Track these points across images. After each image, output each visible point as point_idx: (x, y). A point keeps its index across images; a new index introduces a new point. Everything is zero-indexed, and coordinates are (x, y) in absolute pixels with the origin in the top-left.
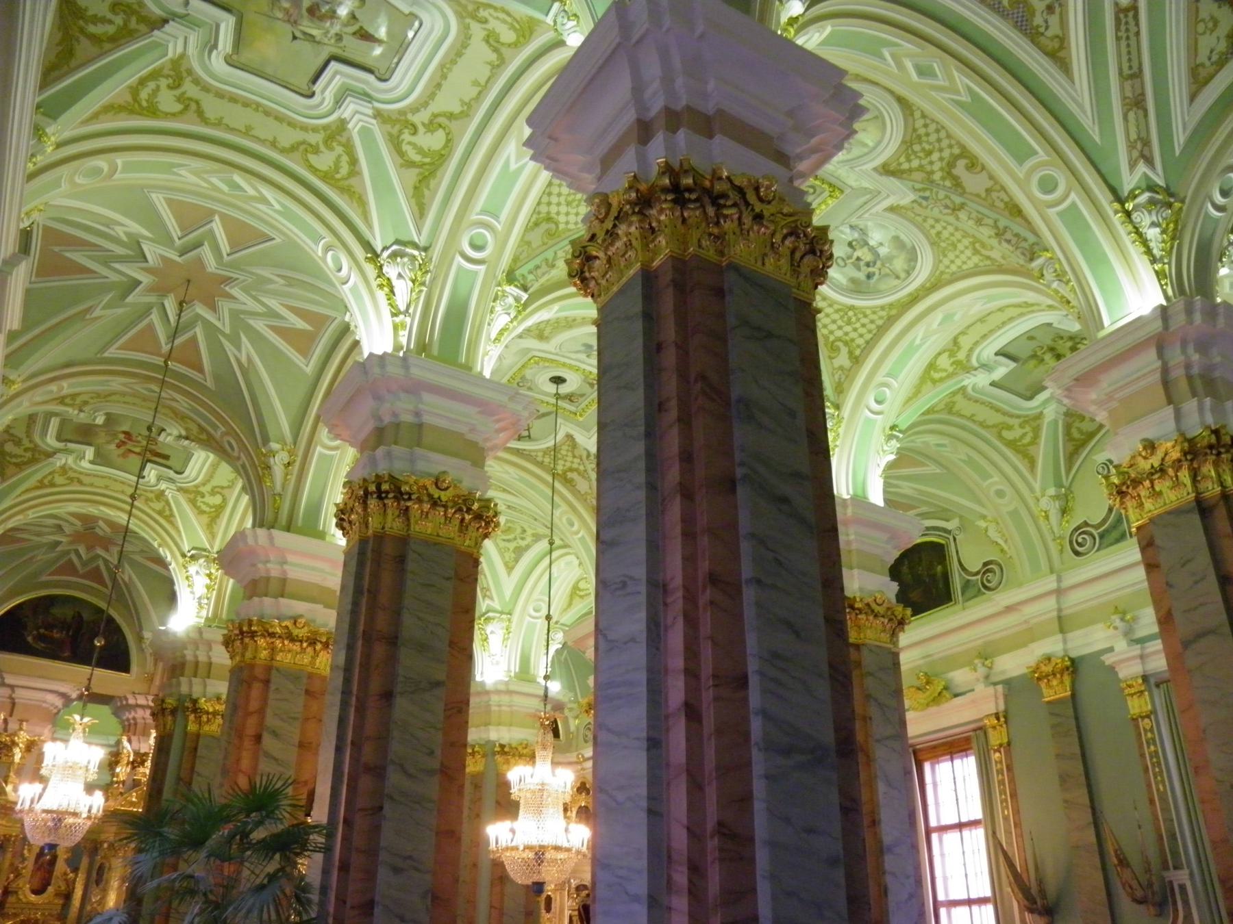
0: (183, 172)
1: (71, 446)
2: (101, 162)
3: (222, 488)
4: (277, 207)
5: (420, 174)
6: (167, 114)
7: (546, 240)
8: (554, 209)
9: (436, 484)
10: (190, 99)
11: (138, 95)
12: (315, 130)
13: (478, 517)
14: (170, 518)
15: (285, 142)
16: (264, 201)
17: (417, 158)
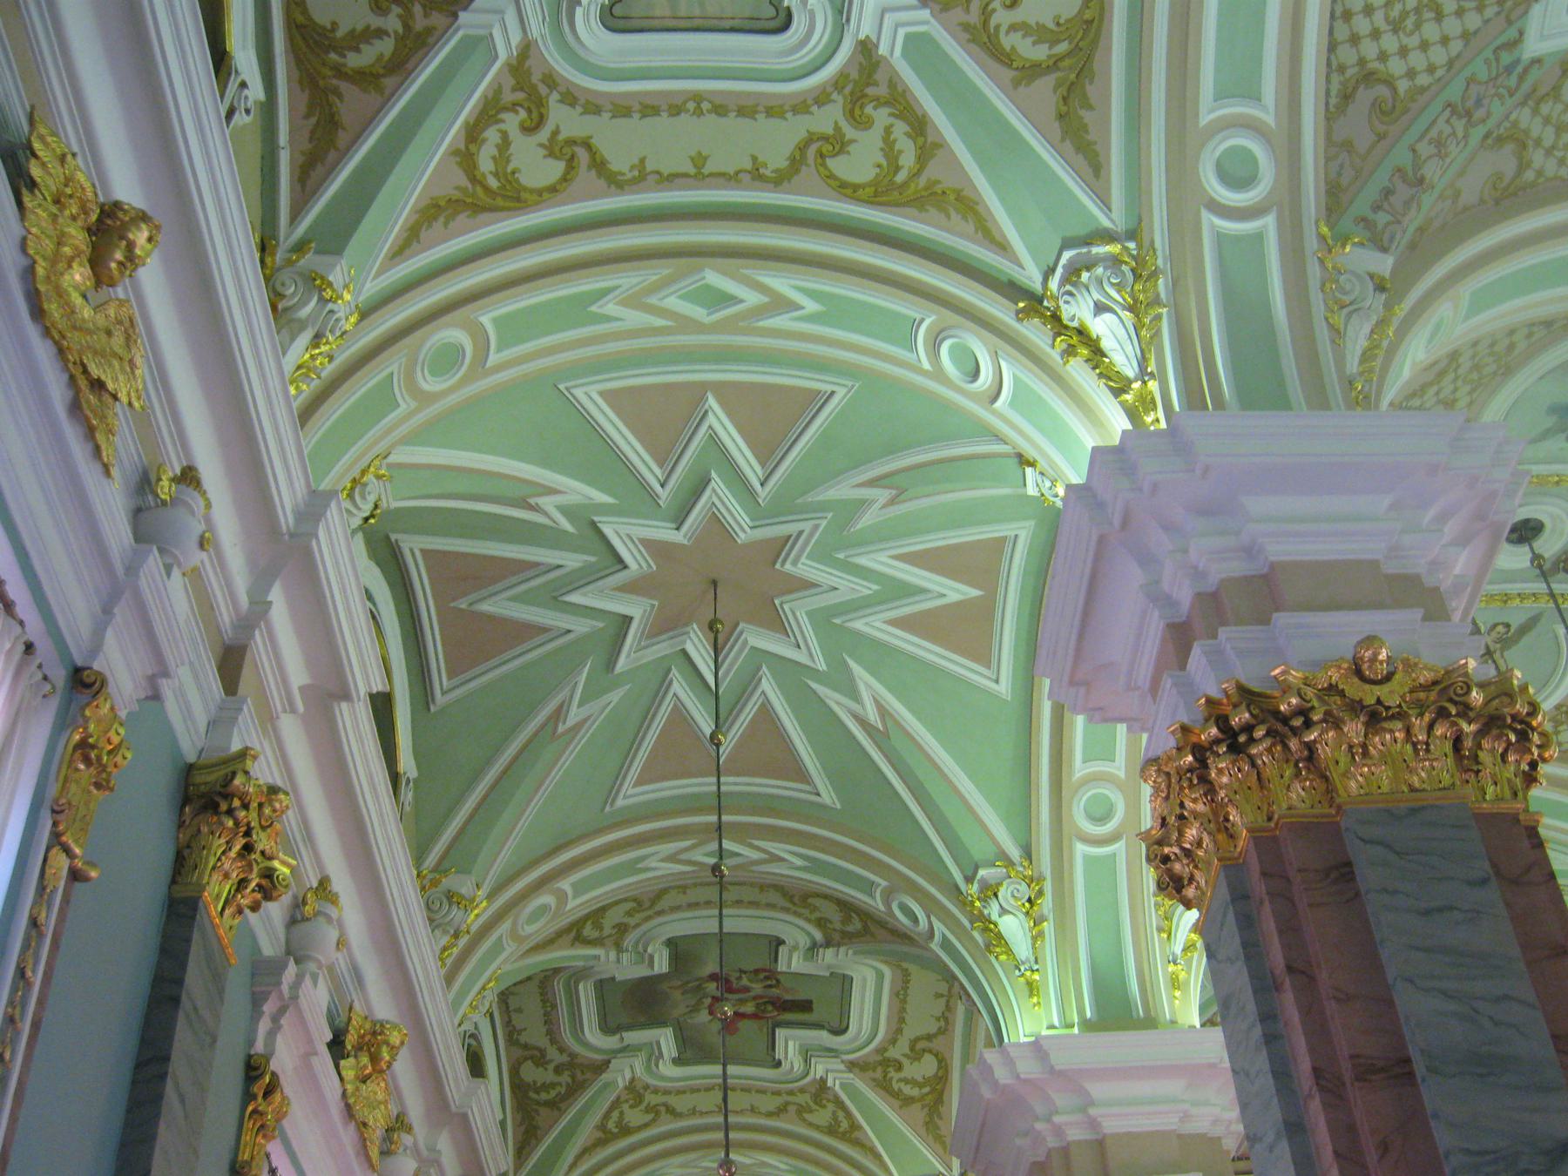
0: (611, 308)
1: (632, 1037)
2: (451, 334)
3: (929, 1037)
4: (811, 306)
5: (1058, 85)
6: (540, 192)
7: (1381, 128)
8: (1369, 49)
9: (1359, 673)
10: (571, 142)
11: (475, 167)
12: (821, 98)
13: (1492, 723)
14: (851, 1134)
15: (776, 160)
16: (781, 304)
17: (1040, 53)
